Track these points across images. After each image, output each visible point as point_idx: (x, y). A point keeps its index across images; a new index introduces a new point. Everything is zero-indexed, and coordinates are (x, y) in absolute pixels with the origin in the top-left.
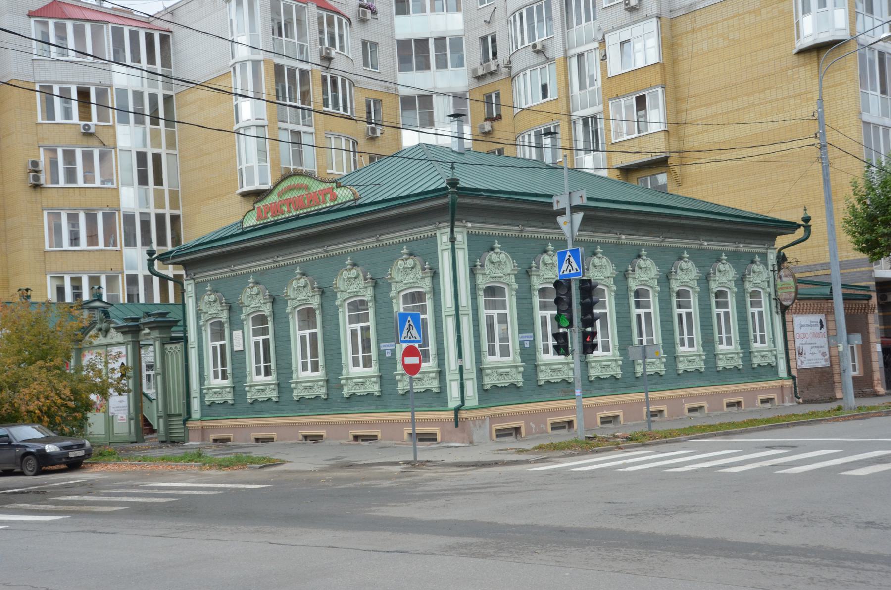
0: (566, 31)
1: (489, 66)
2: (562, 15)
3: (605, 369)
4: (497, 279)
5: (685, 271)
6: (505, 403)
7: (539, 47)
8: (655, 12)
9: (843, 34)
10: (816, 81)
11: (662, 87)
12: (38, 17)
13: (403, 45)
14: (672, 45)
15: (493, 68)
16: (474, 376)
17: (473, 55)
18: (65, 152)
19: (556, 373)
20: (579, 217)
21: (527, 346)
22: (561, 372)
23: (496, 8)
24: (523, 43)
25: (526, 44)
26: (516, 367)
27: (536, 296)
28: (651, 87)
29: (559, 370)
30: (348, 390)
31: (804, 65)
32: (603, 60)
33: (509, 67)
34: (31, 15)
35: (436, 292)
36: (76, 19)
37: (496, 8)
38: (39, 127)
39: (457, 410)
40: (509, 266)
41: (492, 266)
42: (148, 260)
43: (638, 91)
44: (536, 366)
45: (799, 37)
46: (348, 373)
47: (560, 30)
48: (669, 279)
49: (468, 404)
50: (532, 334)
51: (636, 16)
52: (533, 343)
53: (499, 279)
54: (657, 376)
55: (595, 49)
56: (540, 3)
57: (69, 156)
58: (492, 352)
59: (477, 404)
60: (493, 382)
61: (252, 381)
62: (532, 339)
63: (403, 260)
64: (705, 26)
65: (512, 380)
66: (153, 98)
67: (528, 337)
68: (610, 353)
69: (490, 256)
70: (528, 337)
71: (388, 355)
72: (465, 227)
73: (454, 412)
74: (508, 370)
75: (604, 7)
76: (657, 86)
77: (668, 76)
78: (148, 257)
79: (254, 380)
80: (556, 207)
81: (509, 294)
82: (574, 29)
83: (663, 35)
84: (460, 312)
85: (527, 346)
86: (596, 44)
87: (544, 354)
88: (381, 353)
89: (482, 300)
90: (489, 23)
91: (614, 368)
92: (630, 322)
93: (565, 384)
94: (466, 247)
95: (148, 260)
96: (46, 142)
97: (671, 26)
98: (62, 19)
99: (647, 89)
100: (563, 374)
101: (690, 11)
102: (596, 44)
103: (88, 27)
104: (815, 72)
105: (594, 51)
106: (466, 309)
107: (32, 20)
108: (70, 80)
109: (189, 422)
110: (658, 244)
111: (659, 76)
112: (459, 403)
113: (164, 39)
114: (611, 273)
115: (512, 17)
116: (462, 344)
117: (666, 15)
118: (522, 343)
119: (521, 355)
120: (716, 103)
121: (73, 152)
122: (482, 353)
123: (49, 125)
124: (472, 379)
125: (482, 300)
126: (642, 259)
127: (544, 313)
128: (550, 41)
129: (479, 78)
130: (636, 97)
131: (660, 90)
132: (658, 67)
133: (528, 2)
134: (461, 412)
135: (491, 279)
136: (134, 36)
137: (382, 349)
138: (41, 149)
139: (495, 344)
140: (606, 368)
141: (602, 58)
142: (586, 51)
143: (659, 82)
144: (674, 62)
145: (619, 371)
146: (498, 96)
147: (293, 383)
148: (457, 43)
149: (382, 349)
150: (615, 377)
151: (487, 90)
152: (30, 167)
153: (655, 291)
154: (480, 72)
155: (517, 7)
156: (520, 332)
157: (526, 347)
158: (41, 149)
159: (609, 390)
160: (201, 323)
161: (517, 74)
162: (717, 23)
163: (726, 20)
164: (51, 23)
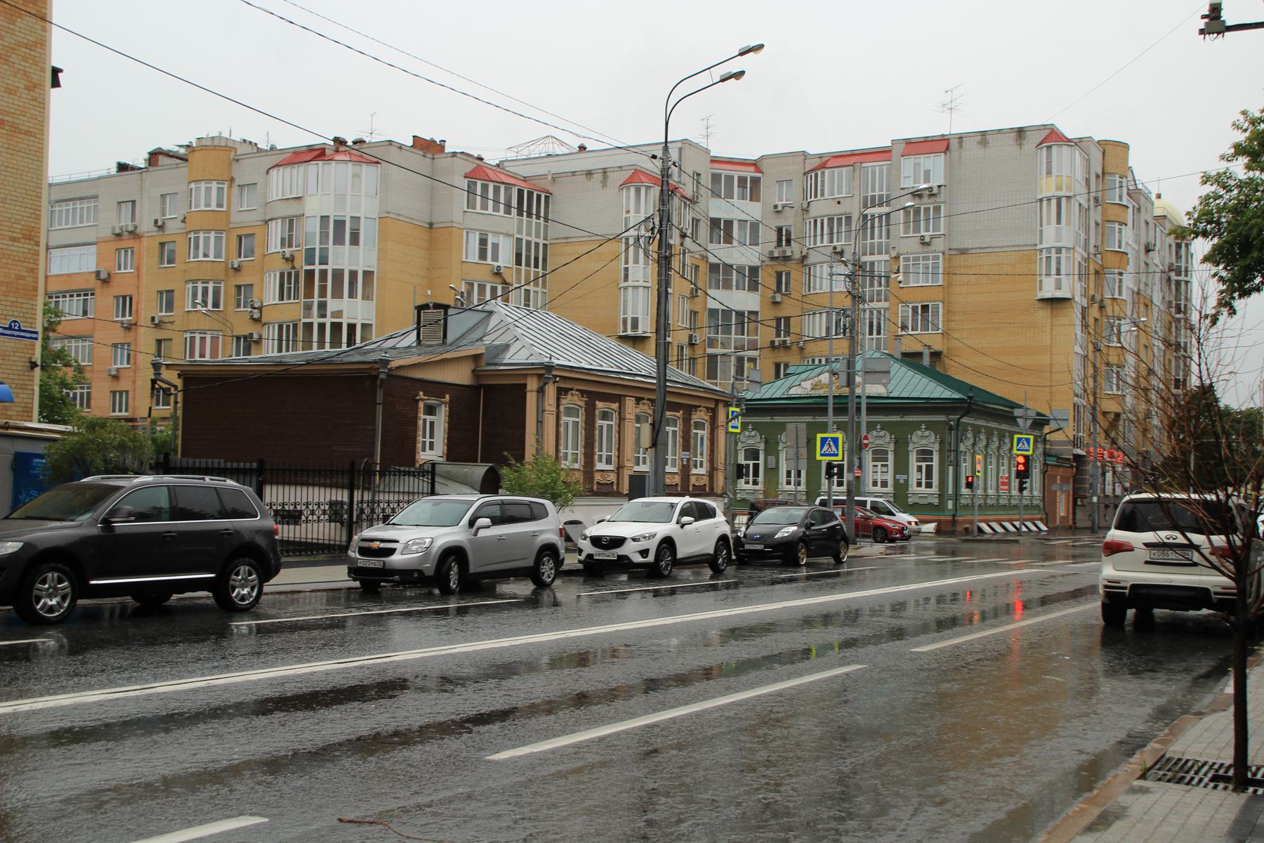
1: (784, 252)
7: (839, 250)
9: (1068, 295)
10: (1049, 320)
13: (715, 223)
15: (788, 254)
17: (768, 236)
18: (479, 285)
20: (1029, 422)
24: (822, 242)
25: (825, 243)
28: (934, 301)
31: (1043, 308)
33: (804, 258)
34: (465, 177)
45: (1041, 289)
51: (926, 248)
57: (482, 288)
66: (537, 245)
71: (902, 482)
80: (1015, 414)
88: (896, 481)
90: (778, 212)
101: (963, 252)
103: (502, 187)
104: (1049, 314)
113: (547, 198)
117: (947, 252)
121: (485, 286)
129: (772, 259)
131: (941, 304)
132: (941, 288)
136: (539, 197)
146: (788, 274)
148: (755, 226)
151: (780, 268)
154: (776, 255)
160: (739, 447)
161: (815, 265)
164: (479, 183)
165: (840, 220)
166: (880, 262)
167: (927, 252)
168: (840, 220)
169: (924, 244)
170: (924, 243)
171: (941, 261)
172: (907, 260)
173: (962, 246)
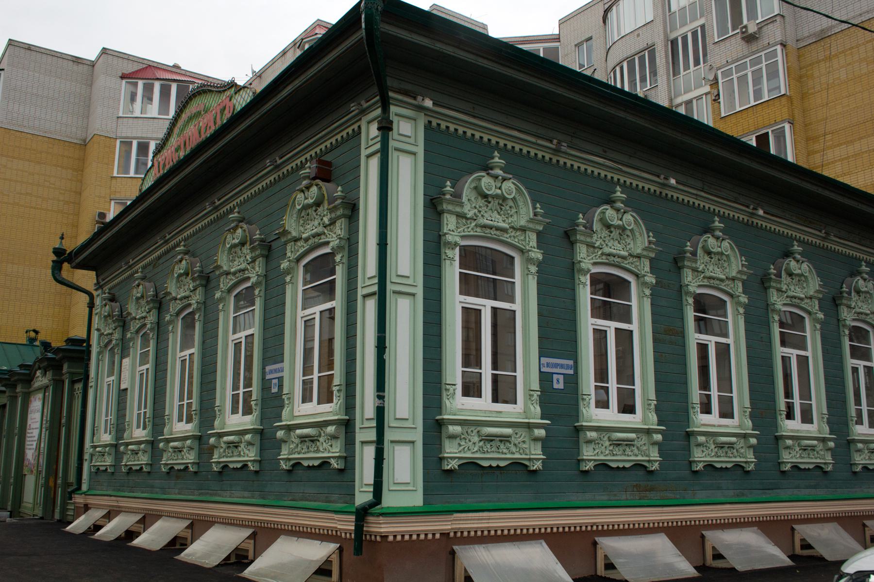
0: (672, 78)
2: (667, 62)
3: (724, 450)
4: (493, 232)
5: (863, 296)
6: (491, 506)
8: (779, 38)
11: (789, 122)
12: (129, 78)
14: (801, 77)
16: (418, 436)
19: (621, 448)
21: (559, 384)
22: (635, 448)
23: (595, 70)
26: (529, 426)
27: (585, 284)
28: (776, 123)
29: (629, 443)
30: (220, 457)
32: (715, 100)
34: (123, 77)
35: (351, 245)
36: (163, 79)
37: (595, 70)
38: (114, 181)
39: (362, 514)
40: (523, 211)
41: (481, 202)
42: (53, 261)
43: (758, 129)
44: (578, 430)
46: (224, 424)
47: (665, 78)
48: (837, 306)
49: (389, 501)
50: (571, 362)
51: (754, 47)
52: (573, 381)
53: (498, 233)
54: (819, 473)
55: (706, 94)
56: (643, 53)
58: (471, 389)
59: (421, 504)
60: (469, 455)
61: (132, 438)
62: (571, 372)
63: (302, 191)
64: (843, 52)
65: (517, 456)
67: (562, 366)
68: (735, 421)
69: (479, 179)
70: (562, 366)
72: (420, 108)
73: (353, 518)
74: (508, 431)
75: (716, 40)
76: (783, 121)
77: (796, 112)
78: (55, 258)
79: (134, 436)
81: (522, 272)
82: (681, 75)
83: (790, 64)
84: (390, 287)
85: (559, 384)
86: (707, 89)
87: (597, 407)
89: (452, 272)
91: (742, 451)
92: (771, 367)
93: (641, 473)
94: (420, 150)
95: (53, 261)
96: (118, 196)
97: (799, 57)
98: (151, 79)
99: (770, 126)
100: (636, 451)
102: (707, 89)
105: (704, 96)
106: (410, 282)
107: (124, 81)
108: (149, 135)
109: (76, 496)
110: (818, 242)
111: (785, 110)
112: (369, 497)
114: (739, 272)
115: (612, 73)
116: (386, 356)
117: (791, 43)
118: (545, 378)
119: (542, 403)
120: (861, 138)
122: (443, 387)
123: (123, 179)
124: (413, 442)
125: (452, 272)
126: (794, 258)
127: (602, 323)
128: (653, 92)
130: (756, 137)
131: (787, 126)
132: (784, 100)
133: (629, 53)
134: (371, 519)
135: (479, 230)
137: (268, 377)
138: (113, 202)
139: (483, 371)
140: (726, 449)
141: (714, 98)
142: (695, 98)
143: (786, 116)
144: (804, 96)
145: (751, 457)
147: (162, 441)
149: (268, 377)
150: (743, 467)
152: (97, 218)
153: (816, 320)
155: (618, 61)
156: (541, 355)
157: (556, 386)
158: (113, 202)
159: (731, 492)
162: (858, 46)
163: (867, 42)
164: (140, 84)
165: (642, 60)
166: (699, 98)
167: (758, 51)
168: (642, 60)
169: (750, 38)
170: (750, 38)
171: (779, 58)
172: (726, 74)
173: (818, 29)
